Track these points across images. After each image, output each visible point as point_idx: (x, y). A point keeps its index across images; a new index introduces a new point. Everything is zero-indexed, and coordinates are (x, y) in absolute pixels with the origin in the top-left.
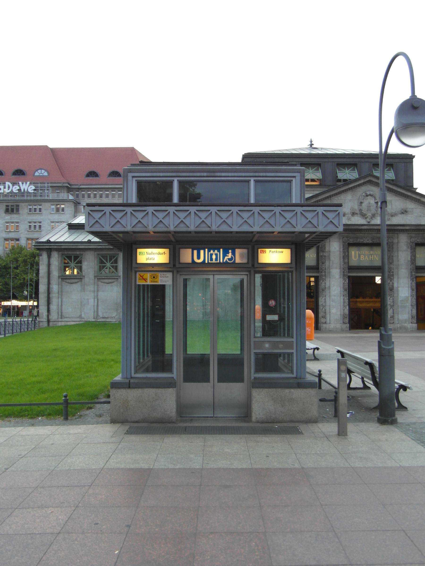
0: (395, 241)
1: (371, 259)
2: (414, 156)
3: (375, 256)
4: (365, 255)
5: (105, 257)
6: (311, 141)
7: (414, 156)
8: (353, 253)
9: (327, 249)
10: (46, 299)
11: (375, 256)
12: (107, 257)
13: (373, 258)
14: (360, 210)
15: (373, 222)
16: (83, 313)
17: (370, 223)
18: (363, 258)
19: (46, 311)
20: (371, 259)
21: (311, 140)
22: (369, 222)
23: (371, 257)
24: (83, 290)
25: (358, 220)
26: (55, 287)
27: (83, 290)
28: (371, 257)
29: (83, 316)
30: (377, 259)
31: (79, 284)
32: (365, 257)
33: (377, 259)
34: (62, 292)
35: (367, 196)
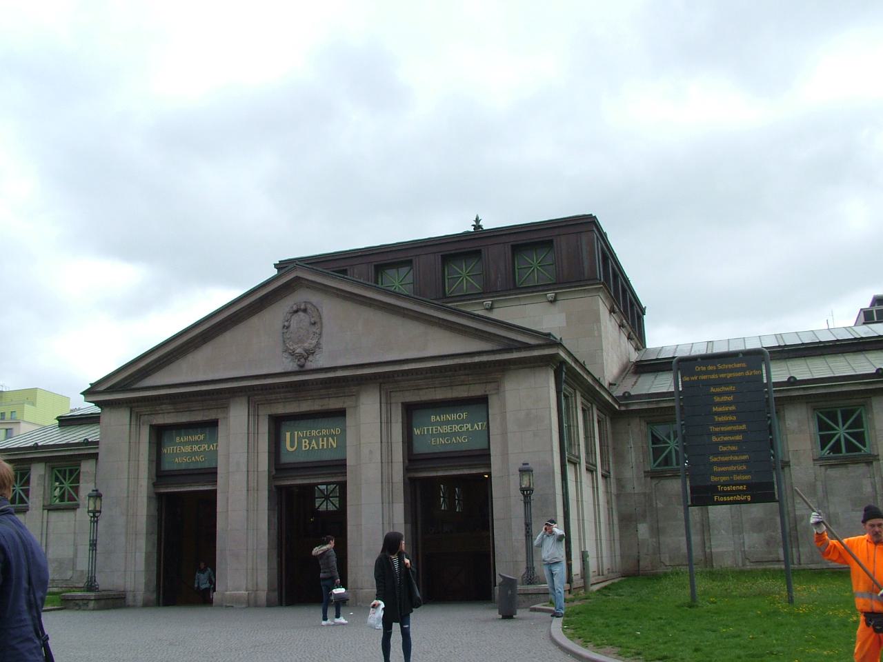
1: (323, 445)
3: (330, 439)
4: (310, 439)
6: (477, 220)
8: (288, 434)
11: (330, 439)
13: (325, 443)
15: (311, 365)
17: (304, 369)
18: (307, 444)
20: (323, 445)
22: (302, 366)
23: (323, 441)
28: (323, 441)
30: (335, 446)
32: (310, 444)
33: (335, 446)
35: (296, 312)
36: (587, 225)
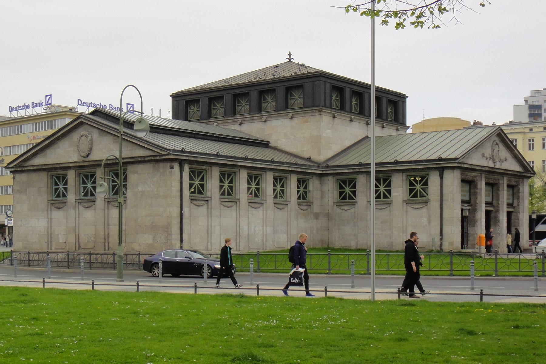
0: (501, 182)
2: (407, 97)
5: (344, 182)
7: (407, 97)
9: (479, 187)
10: (179, 225)
12: (225, 174)
14: (493, 156)
16: (209, 243)
19: (179, 241)
21: (290, 53)
24: (209, 214)
25: (491, 164)
26: (186, 210)
27: (209, 214)
29: (209, 247)
31: (205, 207)
34: (191, 217)
36: (403, 98)
